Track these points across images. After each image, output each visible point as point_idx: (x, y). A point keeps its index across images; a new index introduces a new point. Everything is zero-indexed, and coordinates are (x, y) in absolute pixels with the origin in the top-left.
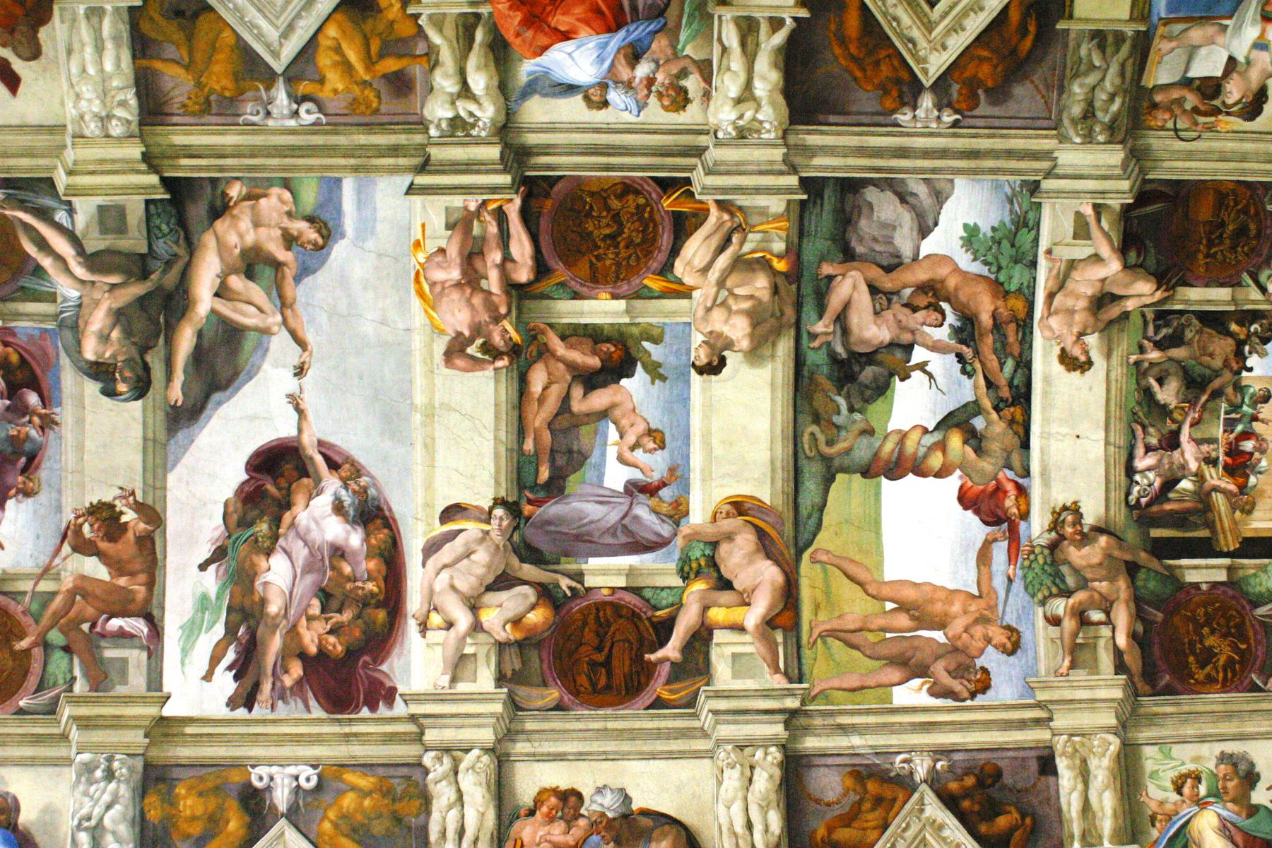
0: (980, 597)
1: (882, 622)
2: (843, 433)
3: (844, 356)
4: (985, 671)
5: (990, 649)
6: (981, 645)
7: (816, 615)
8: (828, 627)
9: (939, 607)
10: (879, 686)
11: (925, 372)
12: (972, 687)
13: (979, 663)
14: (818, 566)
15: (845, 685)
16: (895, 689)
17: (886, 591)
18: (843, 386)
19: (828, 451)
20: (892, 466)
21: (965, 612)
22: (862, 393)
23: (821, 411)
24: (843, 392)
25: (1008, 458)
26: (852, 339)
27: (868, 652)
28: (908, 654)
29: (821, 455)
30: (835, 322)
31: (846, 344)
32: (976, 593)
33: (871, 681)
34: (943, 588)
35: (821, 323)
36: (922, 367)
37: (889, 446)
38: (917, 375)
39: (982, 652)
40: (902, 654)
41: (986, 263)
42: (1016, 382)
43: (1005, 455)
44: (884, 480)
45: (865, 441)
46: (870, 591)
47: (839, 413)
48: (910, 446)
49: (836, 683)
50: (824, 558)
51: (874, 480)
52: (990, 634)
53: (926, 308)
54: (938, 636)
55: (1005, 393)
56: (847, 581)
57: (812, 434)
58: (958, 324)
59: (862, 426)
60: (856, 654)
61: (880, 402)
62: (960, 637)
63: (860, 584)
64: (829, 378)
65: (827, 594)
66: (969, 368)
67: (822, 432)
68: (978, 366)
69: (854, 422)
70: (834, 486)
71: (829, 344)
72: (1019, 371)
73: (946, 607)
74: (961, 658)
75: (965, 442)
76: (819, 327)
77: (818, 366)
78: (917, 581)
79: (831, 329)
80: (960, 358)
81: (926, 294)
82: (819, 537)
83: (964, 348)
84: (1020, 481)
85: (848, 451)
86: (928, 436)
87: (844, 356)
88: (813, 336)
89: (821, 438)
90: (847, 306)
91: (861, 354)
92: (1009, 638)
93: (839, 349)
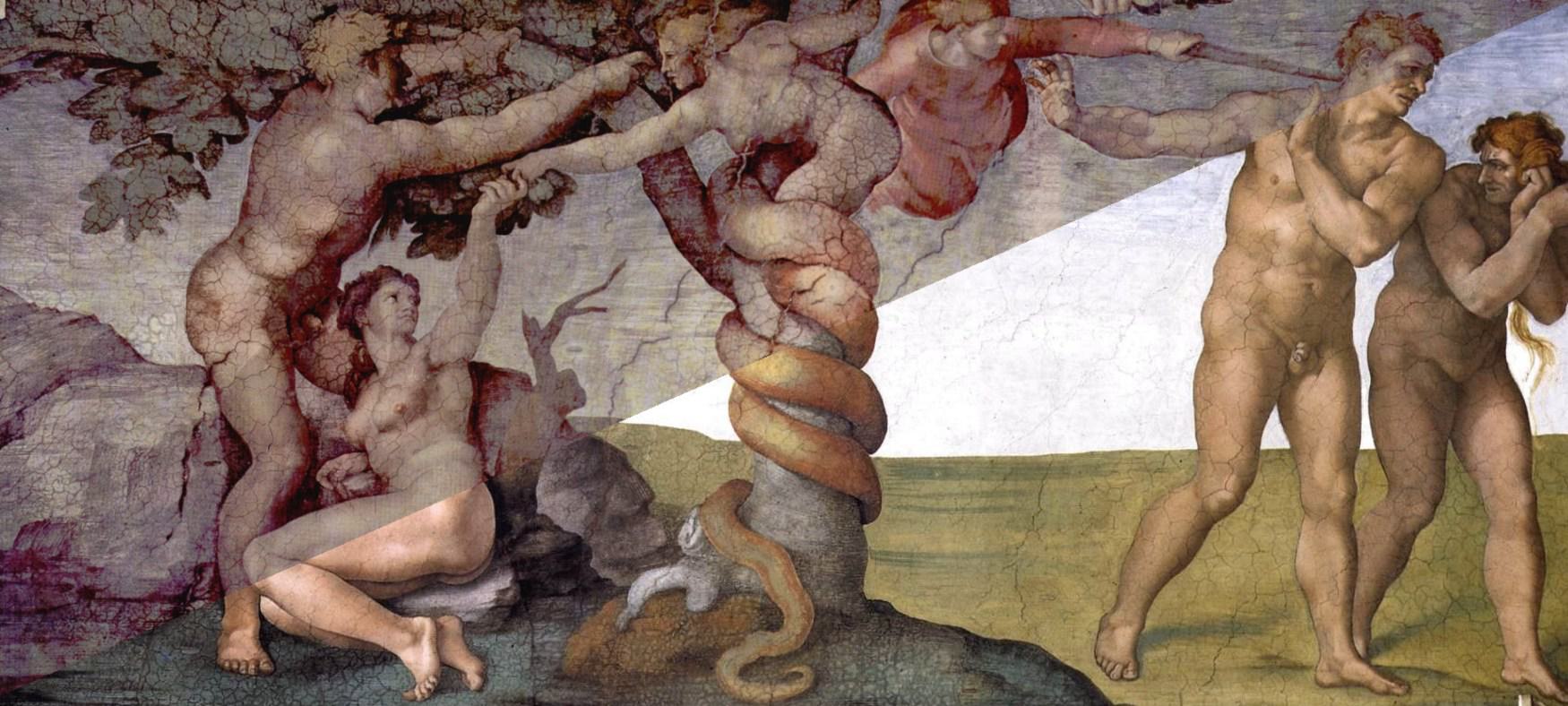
0: (1250, 149)
1: (1323, 465)
2: (742, 576)
3: (505, 581)
4: (1484, 136)
5: (1415, 117)
6: (1402, 146)
7: (1303, 668)
8: (1338, 634)
9: (1282, 282)
10: (1527, 475)
11: (554, 328)
12: (1536, 179)
13: (1461, 154)
14: (1149, 656)
15: (1525, 587)
16: (1539, 427)
17: (1229, 447)
18: (600, 582)
19: (796, 625)
20: (843, 426)
21: (1298, 195)
22: (620, 522)
23: (676, 645)
24: (619, 582)
25: (815, 59)
26: (452, 554)
27: (1420, 509)
28: (1428, 381)
29: (808, 646)
30: (403, 613)
31: (470, 578)
32: (1239, 159)
33: (1511, 502)
34: (1219, 268)
35: (407, 656)
36: (540, 337)
37: (779, 434)
38: (564, 355)
39: (1424, 143)
40: (1429, 405)
41: (211, 157)
42: (584, 40)
43: (807, 70)
44: (890, 449)
45: (765, 510)
46: (1226, 495)
47: (680, 592)
48: (775, 370)
49: (1516, 617)
50: (1123, 637)
51: (886, 480)
52: (1369, 115)
53: (357, 333)
54: (1371, 281)
55: (614, 72)
56: (1195, 569)
57: (745, 672)
58: (407, 233)
59: (718, 521)
60: (1423, 547)
61: (645, 464)
62: (1376, 213)
63: (1205, 525)
64: (572, 622)
65: (1233, 628)
66: (542, 191)
67: (737, 641)
68: (533, 164)
69: (706, 543)
70: (905, 606)
71: (467, 627)
72: (548, 29)
73: (1281, 256)
74: (1442, 208)
75: (770, 195)
76: (420, 660)
77: (535, 660)
78: (1198, 343)
79: (424, 623)
80: (510, 220)
81: (311, 335)
82: (1058, 654)
83: (480, 208)
84: (888, 20)
85: (797, 560)
86: (748, 314)
87: (505, 581)
88: (447, 677)
89: (757, 645)
90: (353, 580)
91: (503, 527)
92: (1384, 55)
93: (485, 596)
